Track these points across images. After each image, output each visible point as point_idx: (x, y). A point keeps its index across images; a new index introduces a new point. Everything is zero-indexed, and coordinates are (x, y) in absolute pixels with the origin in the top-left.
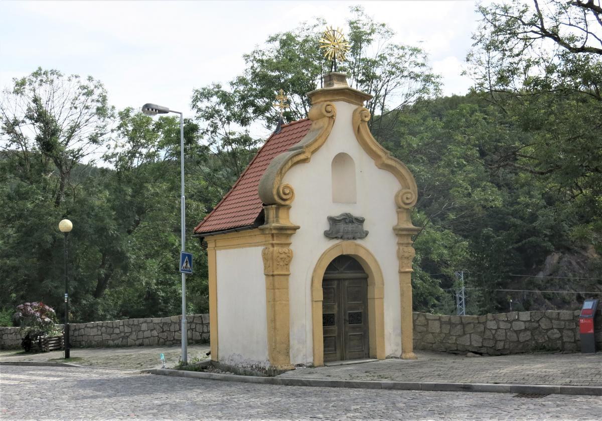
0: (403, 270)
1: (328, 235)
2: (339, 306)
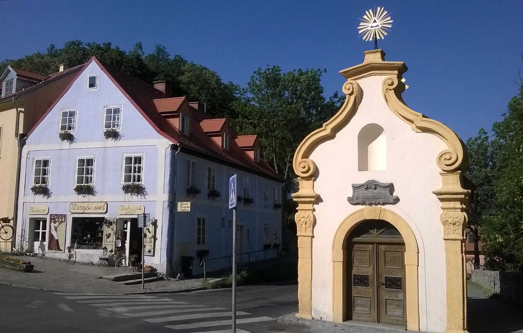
0: (445, 238)
1: (353, 201)
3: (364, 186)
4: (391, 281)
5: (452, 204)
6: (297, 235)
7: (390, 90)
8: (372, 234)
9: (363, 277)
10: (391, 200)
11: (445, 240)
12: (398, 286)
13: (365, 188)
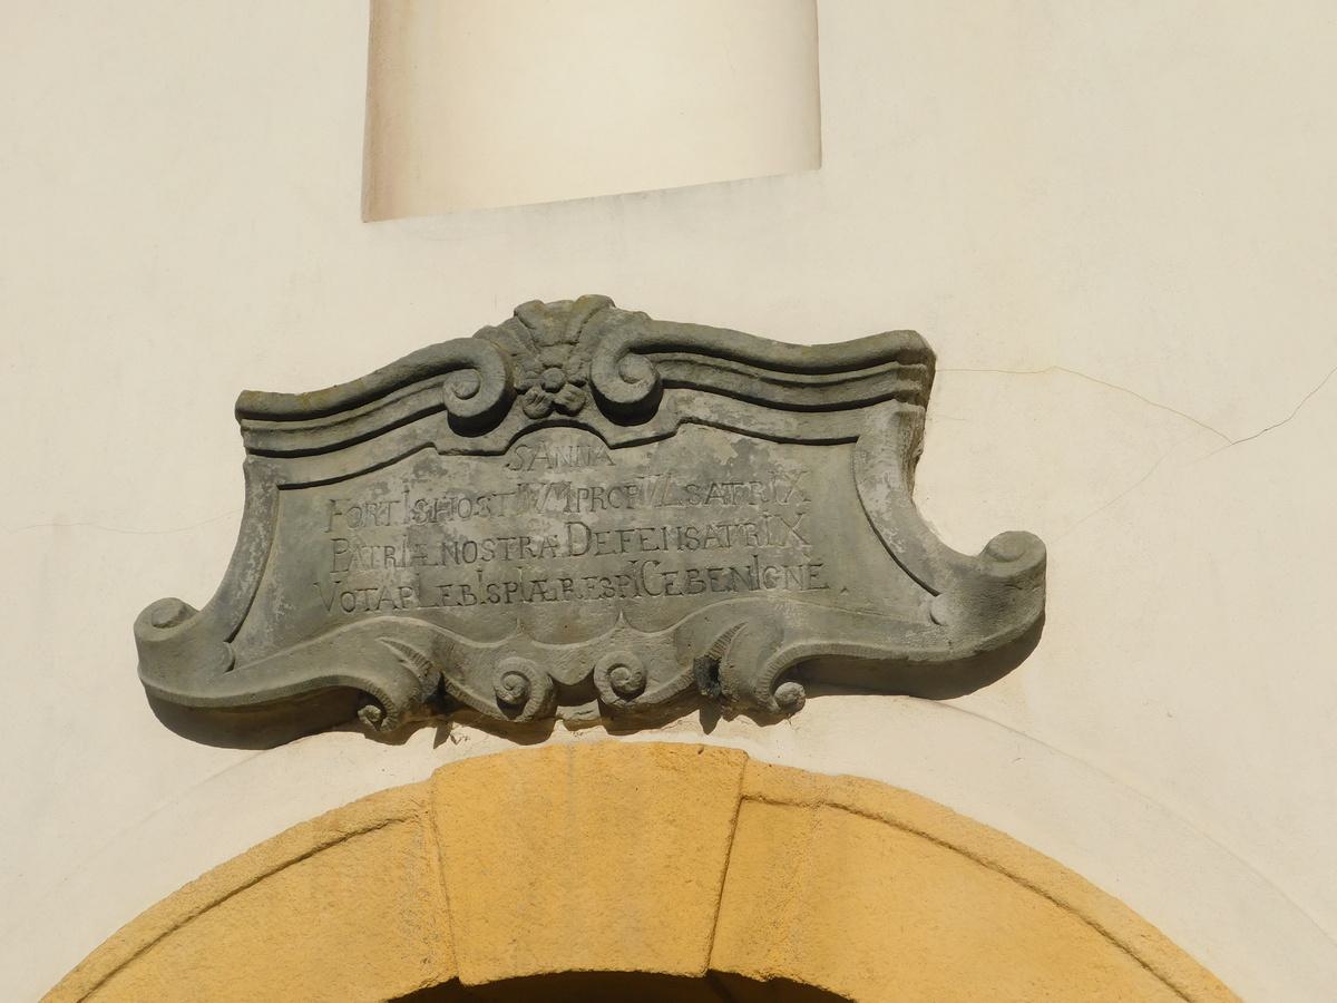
10: (941, 608)
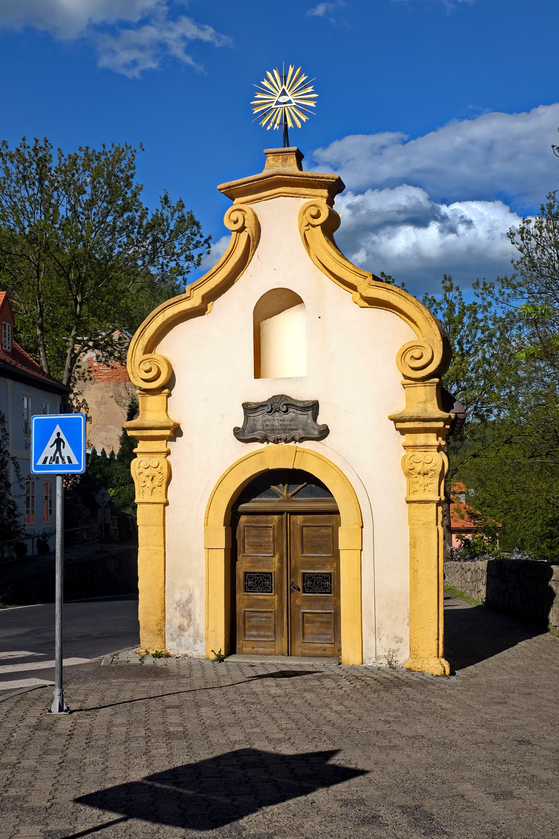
0: (409, 499)
2: (281, 560)
3: (266, 408)
4: (312, 581)
5: (421, 439)
6: (136, 501)
7: (314, 226)
8: (278, 497)
9: (262, 576)
10: (316, 432)
11: (408, 502)
12: (326, 588)
13: (268, 411)
